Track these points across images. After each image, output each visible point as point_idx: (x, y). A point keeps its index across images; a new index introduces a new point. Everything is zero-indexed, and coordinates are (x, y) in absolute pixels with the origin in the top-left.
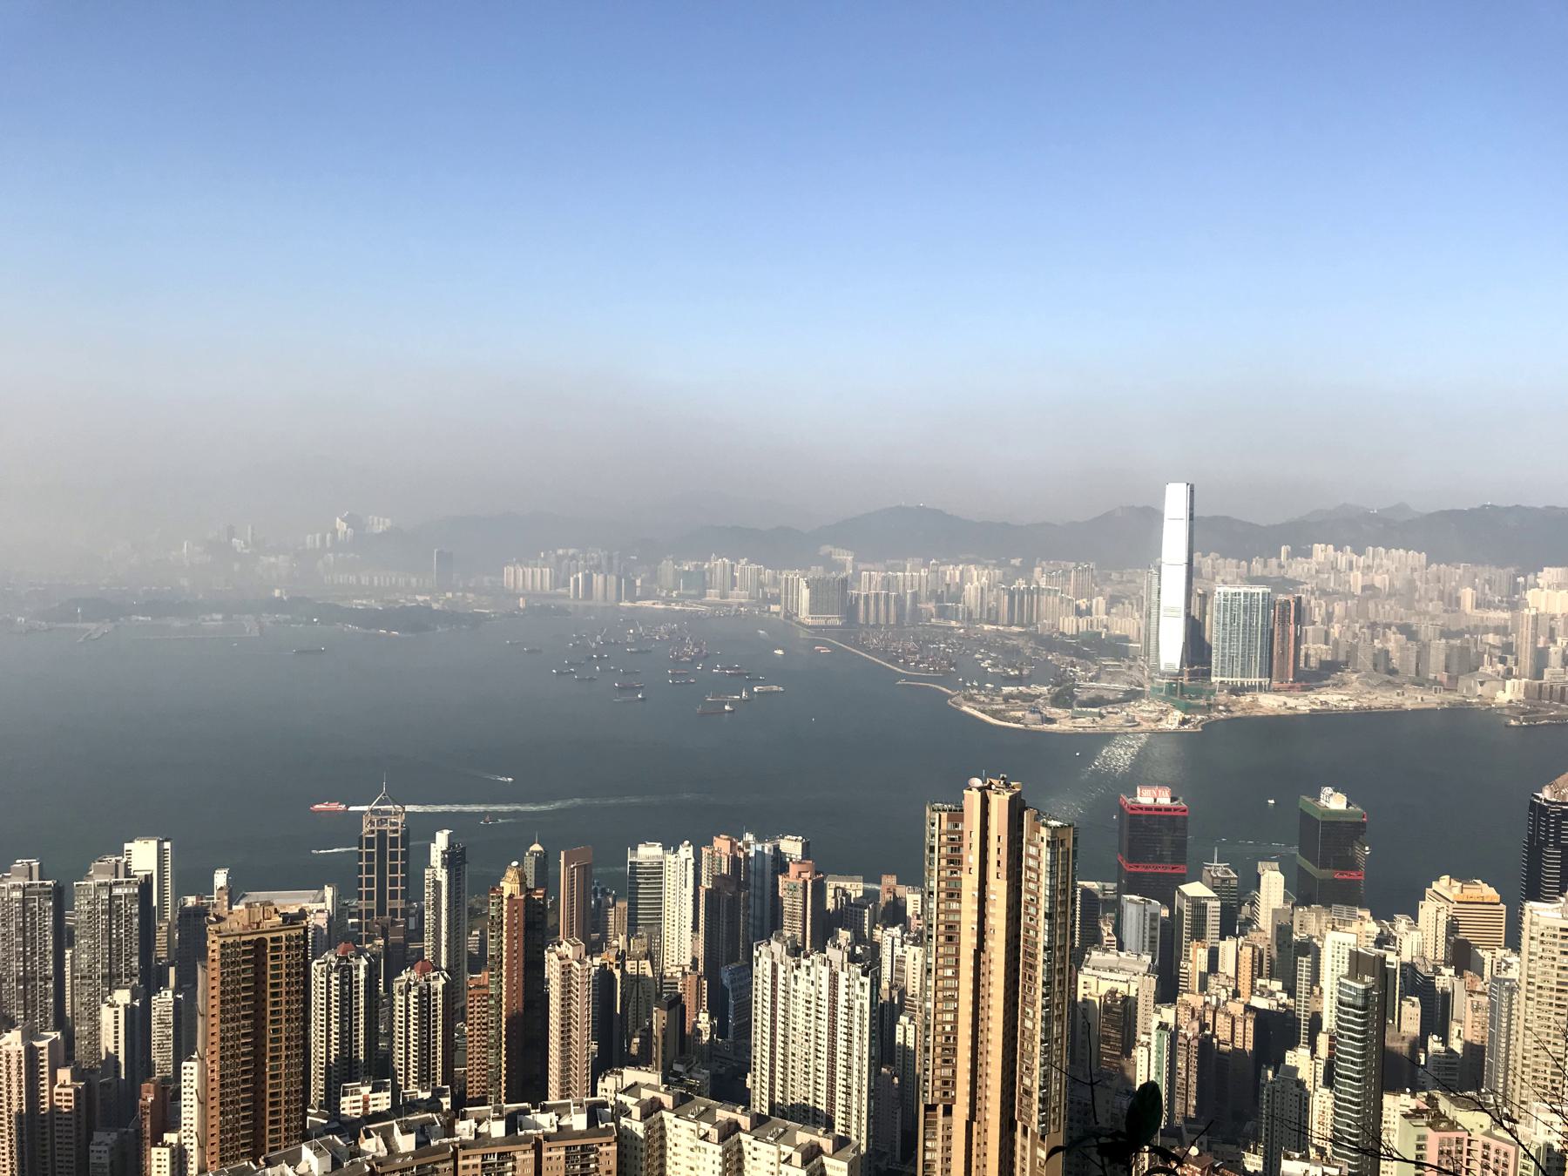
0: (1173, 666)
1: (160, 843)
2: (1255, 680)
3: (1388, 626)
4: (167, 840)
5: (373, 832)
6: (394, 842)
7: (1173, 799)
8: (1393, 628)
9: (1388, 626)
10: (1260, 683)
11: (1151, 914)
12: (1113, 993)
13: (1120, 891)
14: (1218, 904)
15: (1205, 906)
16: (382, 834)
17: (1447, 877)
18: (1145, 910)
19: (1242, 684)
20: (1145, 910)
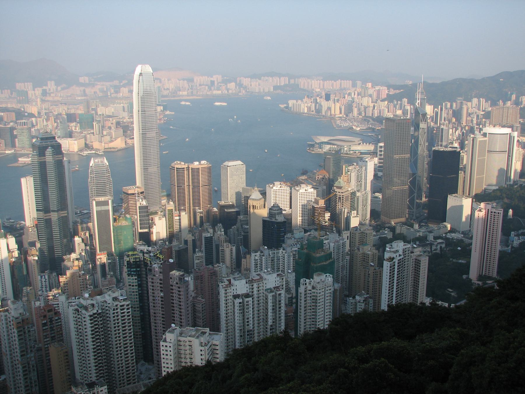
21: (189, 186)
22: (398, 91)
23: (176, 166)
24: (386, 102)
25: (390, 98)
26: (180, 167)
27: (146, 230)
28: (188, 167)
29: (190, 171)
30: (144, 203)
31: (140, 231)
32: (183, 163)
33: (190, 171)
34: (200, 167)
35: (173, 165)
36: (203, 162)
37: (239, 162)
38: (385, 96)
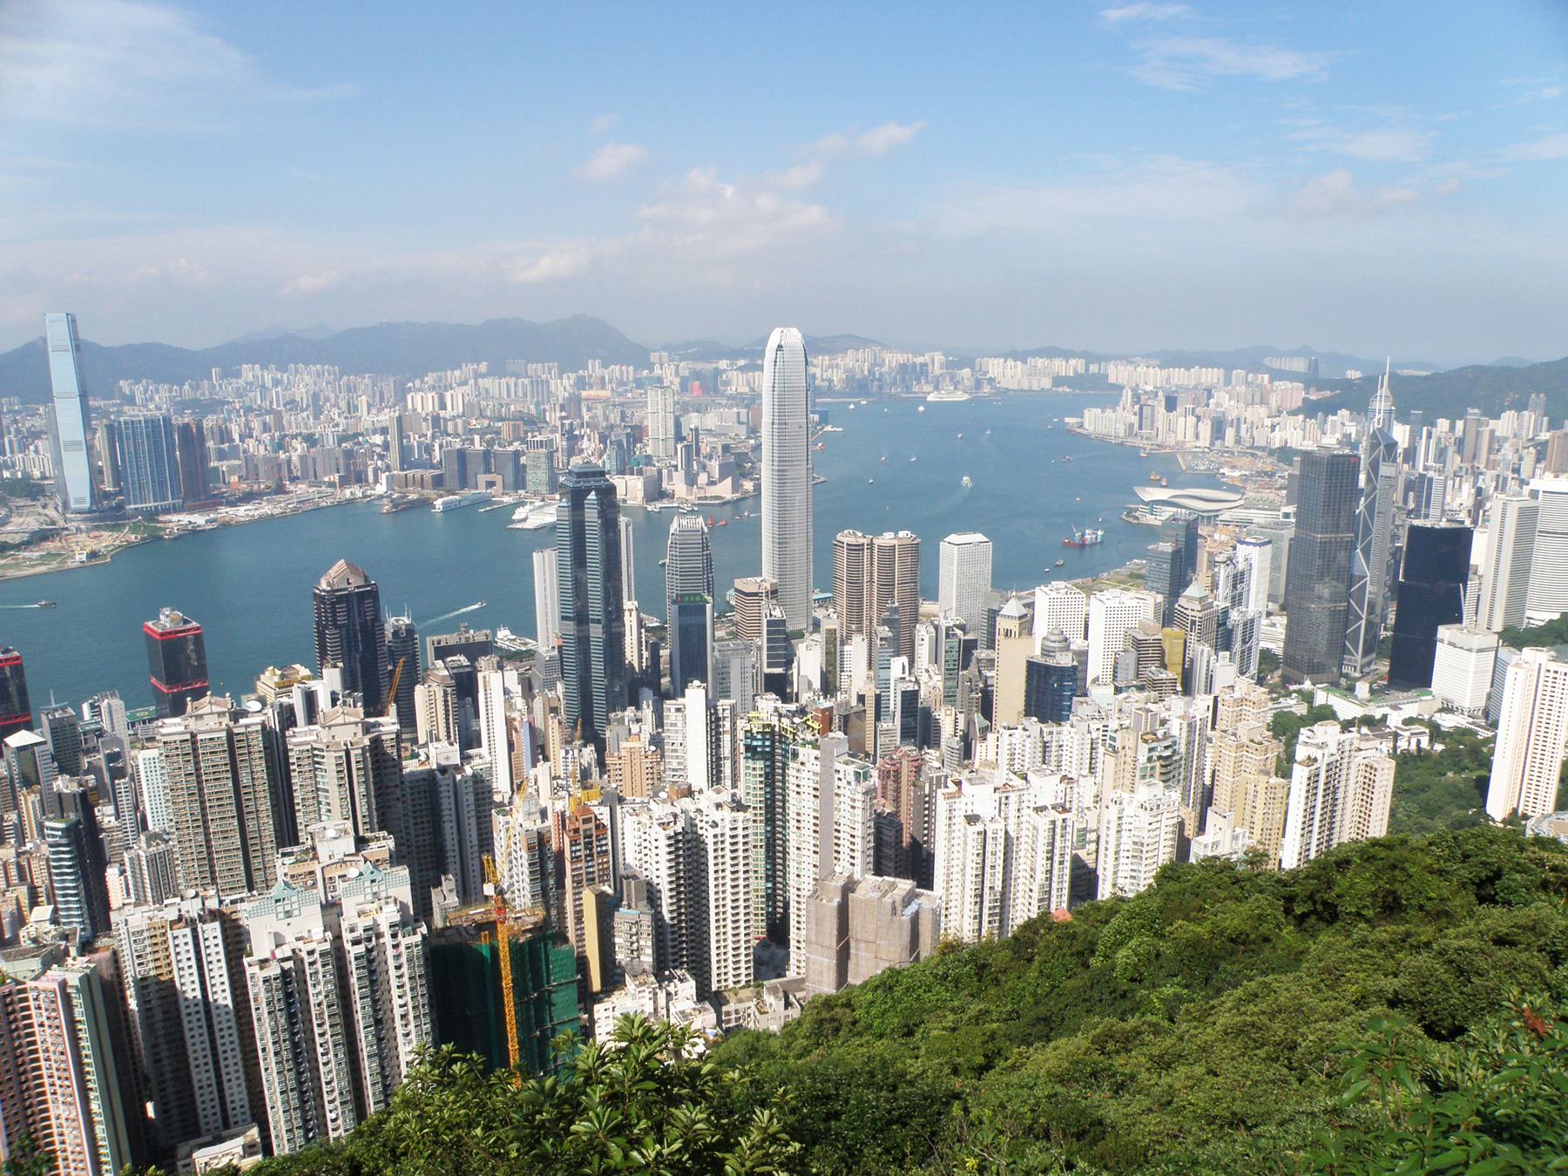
3: (294, 437)
9: (294, 437)
14: (50, 746)
21: (871, 581)
22: (1328, 393)
23: (846, 540)
24: (1301, 417)
25: (1310, 410)
26: (852, 540)
27: (780, 670)
28: (871, 544)
29: (876, 551)
30: (777, 613)
31: (767, 671)
32: (860, 534)
33: (876, 551)
34: (895, 542)
35: (839, 537)
36: (902, 534)
37: (979, 537)
38: (1300, 404)
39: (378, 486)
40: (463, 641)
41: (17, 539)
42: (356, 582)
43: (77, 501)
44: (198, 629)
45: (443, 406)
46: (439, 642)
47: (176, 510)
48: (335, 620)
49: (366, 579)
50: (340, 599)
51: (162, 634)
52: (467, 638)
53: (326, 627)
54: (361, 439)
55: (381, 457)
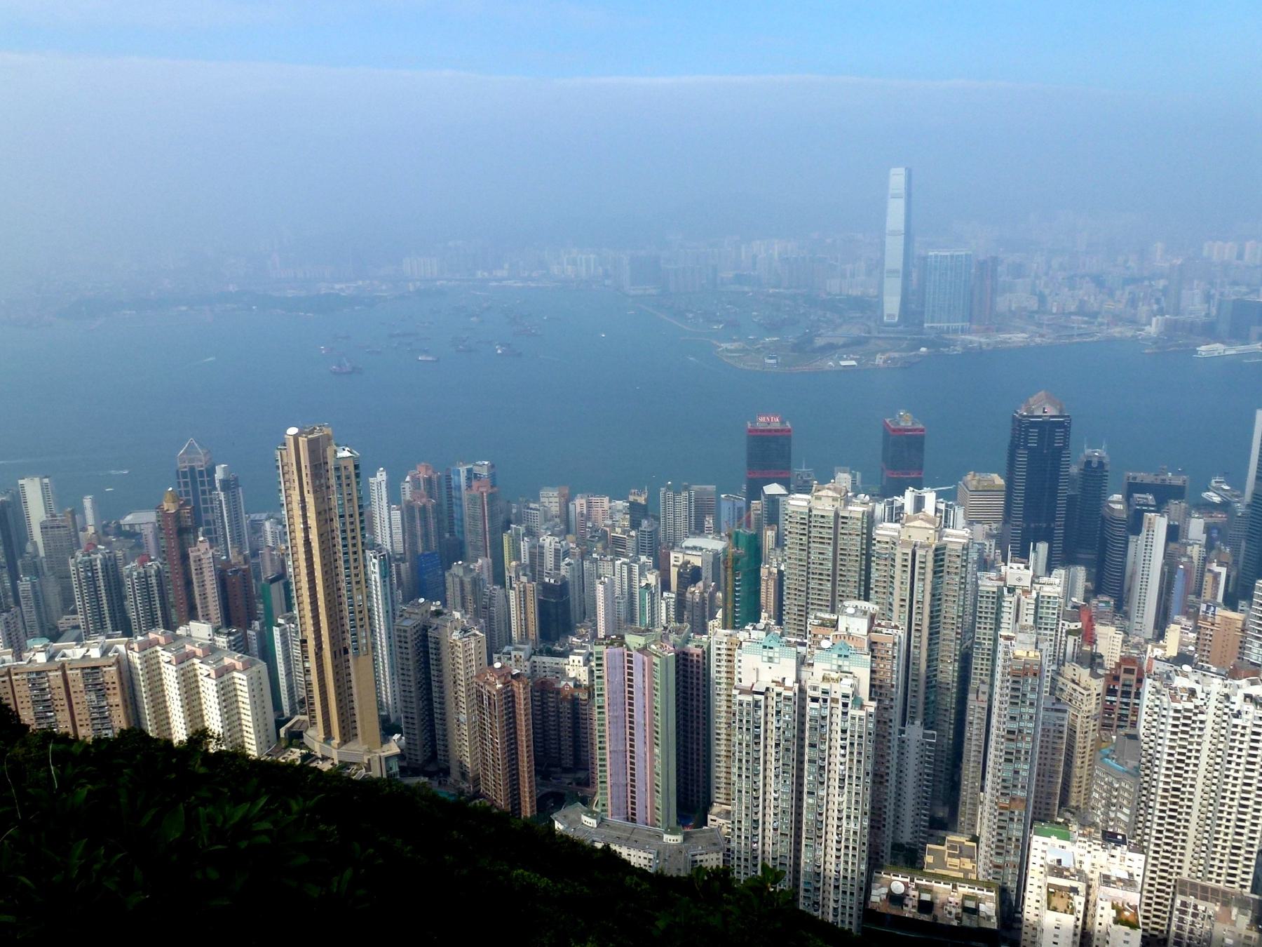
0: (894, 316)
1: (41, 479)
2: (959, 325)
3: (1083, 277)
4: (46, 477)
5: (185, 467)
6: (201, 473)
7: (782, 422)
8: (1087, 279)
9: (1083, 277)
10: (962, 326)
11: (738, 508)
12: (686, 563)
13: (719, 492)
15: (778, 500)
16: (192, 469)
17: (972, 473)
18: (734, 505)
19: (948, 327)
20: (734, 505)
39: (1147, 328)
40: (1159, 482)
41: (841, 341)
42: (1051, 411)
43: (889, 316)
44: (922, 430)
45: (1240, 256)
46: (1135, 478)
47: (963, 331)
48: (1026, 442)
49: (1061, 412)
50: (1034, 424)
51: (894, 430)
52: (1164, 480)
53: (1017, 447)
54: (1146, 283)
55: (1158, 301)
